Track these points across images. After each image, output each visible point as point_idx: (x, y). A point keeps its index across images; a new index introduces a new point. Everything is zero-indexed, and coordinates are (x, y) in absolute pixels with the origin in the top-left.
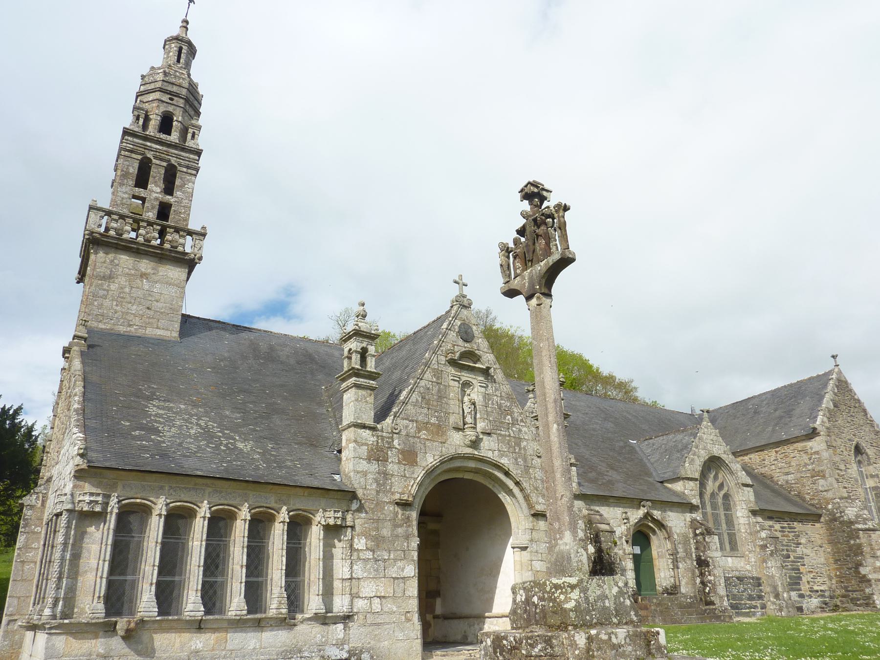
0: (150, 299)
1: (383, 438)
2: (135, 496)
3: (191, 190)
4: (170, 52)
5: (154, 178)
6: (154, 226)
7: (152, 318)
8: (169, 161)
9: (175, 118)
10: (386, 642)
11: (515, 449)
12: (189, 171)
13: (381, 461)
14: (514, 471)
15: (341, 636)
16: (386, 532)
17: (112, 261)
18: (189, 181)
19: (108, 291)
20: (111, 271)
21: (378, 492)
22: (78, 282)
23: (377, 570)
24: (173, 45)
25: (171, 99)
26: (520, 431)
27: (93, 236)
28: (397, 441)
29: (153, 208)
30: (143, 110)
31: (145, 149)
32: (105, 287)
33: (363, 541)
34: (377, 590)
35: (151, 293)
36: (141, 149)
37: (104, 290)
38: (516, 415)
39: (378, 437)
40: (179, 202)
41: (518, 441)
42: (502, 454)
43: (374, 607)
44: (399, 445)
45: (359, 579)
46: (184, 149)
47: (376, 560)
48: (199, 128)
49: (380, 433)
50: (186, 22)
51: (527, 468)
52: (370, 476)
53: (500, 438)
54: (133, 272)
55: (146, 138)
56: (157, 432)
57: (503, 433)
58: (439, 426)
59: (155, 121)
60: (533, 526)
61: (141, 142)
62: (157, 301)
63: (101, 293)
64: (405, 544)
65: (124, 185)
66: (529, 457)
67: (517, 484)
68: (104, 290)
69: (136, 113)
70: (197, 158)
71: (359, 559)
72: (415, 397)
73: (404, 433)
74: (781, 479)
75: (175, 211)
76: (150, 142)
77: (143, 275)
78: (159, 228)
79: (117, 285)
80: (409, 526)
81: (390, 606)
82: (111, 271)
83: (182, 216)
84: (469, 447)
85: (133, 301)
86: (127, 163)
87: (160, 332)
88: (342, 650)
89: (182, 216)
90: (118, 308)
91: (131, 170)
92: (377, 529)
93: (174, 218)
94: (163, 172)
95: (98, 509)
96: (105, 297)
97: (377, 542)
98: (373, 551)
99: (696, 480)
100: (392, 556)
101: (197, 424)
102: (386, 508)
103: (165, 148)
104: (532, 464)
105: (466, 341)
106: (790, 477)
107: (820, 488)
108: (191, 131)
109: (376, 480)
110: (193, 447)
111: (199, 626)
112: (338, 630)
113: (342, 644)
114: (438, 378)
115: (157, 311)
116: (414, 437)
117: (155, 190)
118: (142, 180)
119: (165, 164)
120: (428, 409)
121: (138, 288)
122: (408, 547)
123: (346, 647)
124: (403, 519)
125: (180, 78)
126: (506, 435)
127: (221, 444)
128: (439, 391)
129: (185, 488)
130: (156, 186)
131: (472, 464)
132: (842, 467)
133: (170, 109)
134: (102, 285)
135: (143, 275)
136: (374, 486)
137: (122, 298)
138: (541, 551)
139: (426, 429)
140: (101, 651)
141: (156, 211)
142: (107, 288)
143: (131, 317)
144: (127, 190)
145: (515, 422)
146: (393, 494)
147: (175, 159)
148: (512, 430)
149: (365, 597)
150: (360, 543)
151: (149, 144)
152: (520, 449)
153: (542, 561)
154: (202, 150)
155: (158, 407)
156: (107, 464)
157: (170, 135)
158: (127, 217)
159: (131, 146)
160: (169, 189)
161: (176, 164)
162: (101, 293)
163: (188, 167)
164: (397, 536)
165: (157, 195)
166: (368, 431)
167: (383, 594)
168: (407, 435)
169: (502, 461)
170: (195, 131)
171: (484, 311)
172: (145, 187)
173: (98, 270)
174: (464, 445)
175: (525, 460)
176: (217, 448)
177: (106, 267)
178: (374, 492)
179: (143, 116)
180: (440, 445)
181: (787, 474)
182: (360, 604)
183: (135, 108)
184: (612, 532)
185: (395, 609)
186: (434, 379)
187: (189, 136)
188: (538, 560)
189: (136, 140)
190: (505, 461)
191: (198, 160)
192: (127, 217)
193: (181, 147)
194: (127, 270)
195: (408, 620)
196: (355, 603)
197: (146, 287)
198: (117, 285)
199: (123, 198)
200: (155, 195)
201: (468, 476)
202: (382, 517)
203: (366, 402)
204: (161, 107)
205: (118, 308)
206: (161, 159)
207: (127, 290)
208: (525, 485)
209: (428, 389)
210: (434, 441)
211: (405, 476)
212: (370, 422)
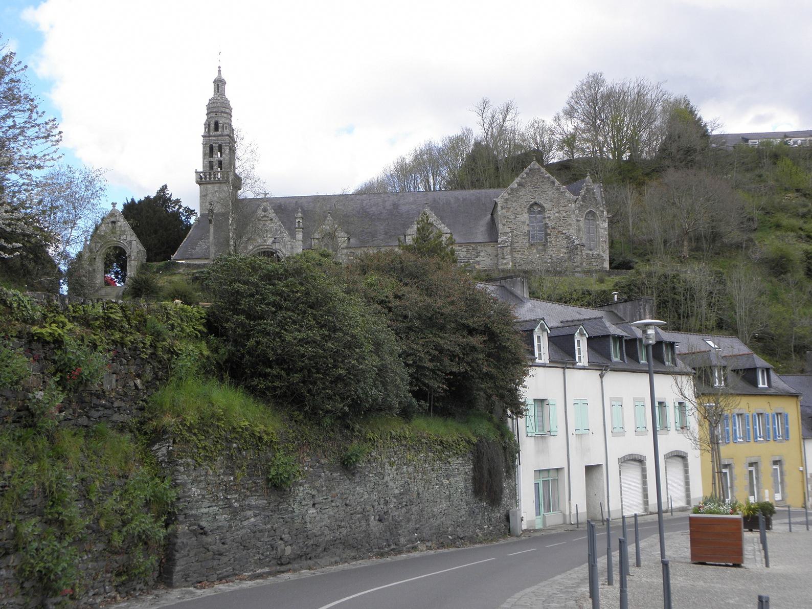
46: (223, 136)
51: (285, 246)
55: (209, 136)
59: (213, 126)
125: (218, 102)
133: (216, 119)
145: (281, 233)
160: (211, 163)
172: (212, 157)
208: (284, 251)
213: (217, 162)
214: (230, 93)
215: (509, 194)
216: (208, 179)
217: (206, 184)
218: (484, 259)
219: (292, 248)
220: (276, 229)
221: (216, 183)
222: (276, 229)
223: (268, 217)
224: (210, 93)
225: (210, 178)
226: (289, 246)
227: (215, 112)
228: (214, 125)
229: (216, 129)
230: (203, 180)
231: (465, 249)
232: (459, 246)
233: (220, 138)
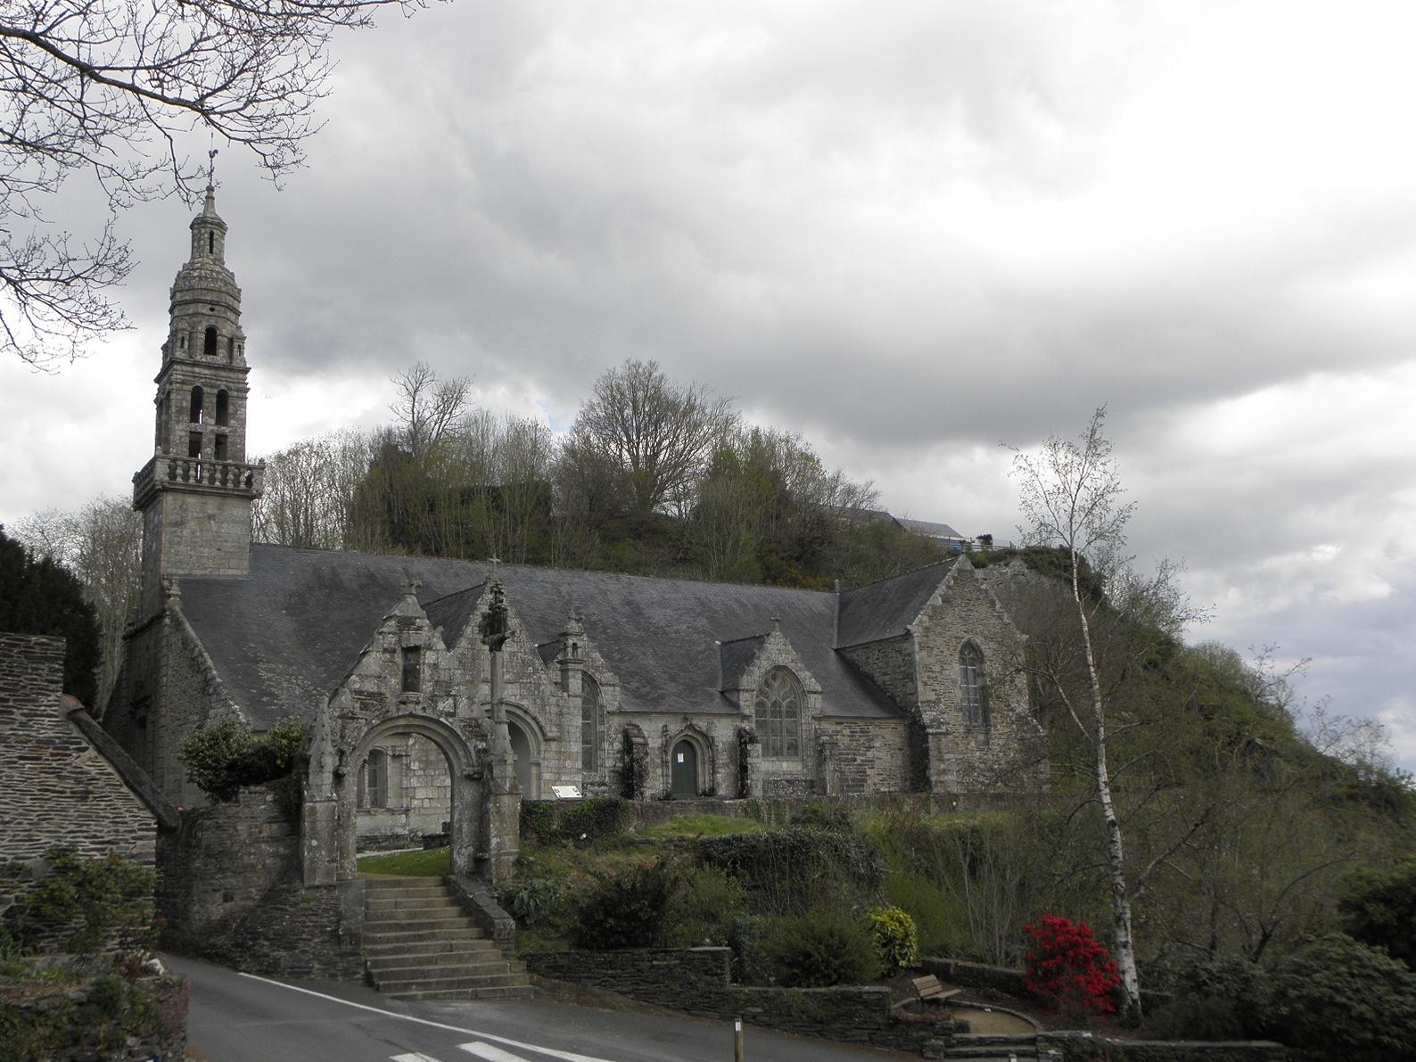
14: (532, 709)
15: (404, 821)
16: (432, 758)
17: (181, 507)
19: (181, 537)
24: (203, 231)
25: (212, 310)
29: (210, 442)
32: (179, 534)
33: (417, 764)
41: (538, 686)
46: (232, 370)
54: (201, 515)
55: (195, 364)
61: (190, 369)
62: (226, 541)
63: (176, 540)
67: (534, 719)
74: (880, 679)
77: (210, 517)
78: (220, 467)
86: (179, 397)
87: (231, 572)
90: (192, 553)
91: (185, 404)
92: (427, 756)
94: (215, 400)
96: (179, 543)
97: (427, 764)
99: (753, 691)
103: (213, 372)
106: (887, 678)
107: (908, 692)
108: (236, 344)
117: (207, 422)
119: (216, 391)
121: (207, 530)
125: (217, 279)
128: (473, 655)
130: (210, 417)
132: (937, 668)
133: (212, 322)
134: (175, 532)
135: (210, 517)
143: (205, 561)
145: (536, 671)
150: (415, 766)
151: (197, 370)
157: (215, 354)
162: (176, 540)
163: (238, 390)
171: (645, 364)
175: (542, 700)
181: (885, 674)
182: (415, 803)
184: (646, 744)
187: (236, 350)
189: (184, 368)
190: (525, 703)
193: (229, 368)
197: (214, 529)
200: (210, 428)
205: (192, 553)
206: (212, 386)
207: (198, 534)
213: (213, 437)
214: (237, 259)
215: (931, 618)
216: (205, 482)
217: (184, 492)
218: (881, 755)
219: (560, 714)
221: (211, 494)
225: (224, 482)
226: (554, 710)
227: (211, 303)
228: (203, 336)
229: (211, 347)
230: (179, 479)
231: (847, 732)
232: (837, 723)
233: (223, 374)
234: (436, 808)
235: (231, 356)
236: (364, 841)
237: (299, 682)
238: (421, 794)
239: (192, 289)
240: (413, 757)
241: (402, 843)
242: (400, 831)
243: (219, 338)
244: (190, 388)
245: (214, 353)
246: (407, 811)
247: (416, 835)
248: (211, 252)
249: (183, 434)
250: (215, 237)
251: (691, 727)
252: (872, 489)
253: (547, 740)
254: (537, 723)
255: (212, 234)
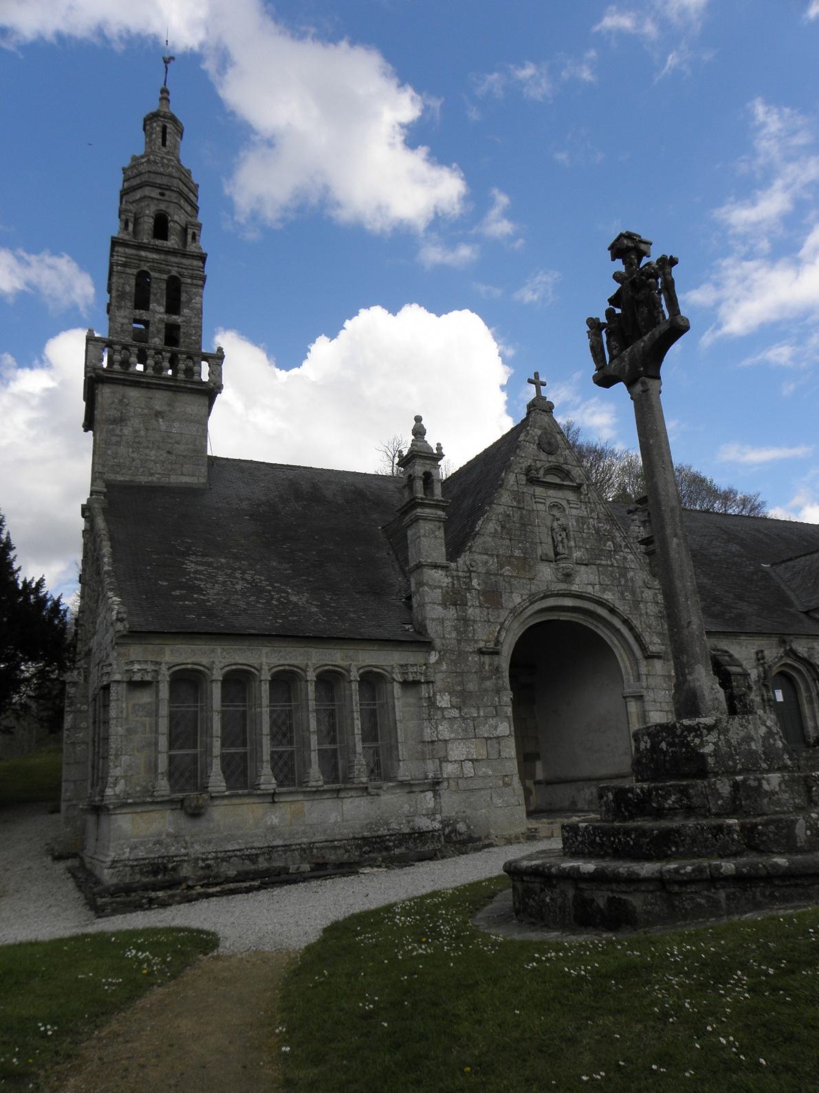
0: (170, 441)
1: (458, 577)
2: (185, 661)
3: (199, 306)
4: (152, 134)
5: (155, 295)
6: (164, 353)
7: (175, 463)
8: (169, 271)
9: (169, 218)
10: (483, 811)
11: (620, 582)
12: (195, 281)
13: (459, 605)
14: (621, 607)
15: (431, 804)
16: (471, 686)
17: (121, 401)
18: (196, 294)
20: (122, 413)
21: (459, 641)
22: (86, 430)
23: (465, 730)
25: (162, 194)
26: (625, 558)
27: (96, 374)
28: (476, 580)
29: (159, 331)
30: (131, 212)
31: (141, 260)
32: (118, 432)
33: (447, 697)
34: (468, 753)
35: (170, 434)
36: (135, 261)
37: (117, 436)
38: (618, 539)
39: (453, 577)
40: (188, 322)
41: (624, 571)
42: (604, 588)
43: (465, 772)
44: (479, 585)
45: (445, 741)
46: (184, 255)
47: (464, 719)
48: (199, 226)
49: (455, 573)
50: (164, 91)
51: (636, 604)
52: (448, 623)
53: (600, 569)
54: (146, 411)
55: (140, 247)
56: (200, 590)
57: (604, 562)
58: (525, 559)
59: (148, 224)
60: (648, 670)
61: (133, 252)
62: (178, 443)
63: (114, 439)
64: (496, 699)
65: (122, 307)
66: (638, 590)
67: (626, 622)
68: (117, 436)
69: (123, 217)
70: (201, 264)
71: (444, 718)
72: (492, 526)
73: (482, 570)
75: (184, 333)
76: (144, 251)
77: (158, 414)
79: (130, 428)
80: (499, 678)
81: (484, 770)
82: (122, 413)
83: (193, 338)
84: (562, 582)
85: (151, 445)
87: (185, 479)
88: (434, 820)
89: (193, 338)
90: (135, 455)
91: (128, 289)
92: (462, 683)
93: (184, 341)
94: (164, 286)
95: (148, 678)
96: (118, 444)
97: (463, 698)
98: (460, 709)
100: (482, 714)
101: (243, 579)
102: (470, 658)
103: (163, 257)
104: (642, 597)
105: (550, 453)
108: (190, 231)
109: (456, 628)
110: (242, 605)
111: (273, 797)
112: (428, 798)
113: (434, 814)
114: (519, 502)
115: (180, 455)
116: (496, 575)
117: (158, 310)
118: (142, 302)
119: (165, 277)
120: (510, 540)
121: (154, 429)
122: (500, 701)
123: (438, 817)
124: (491, 671)
126: (608, 566)
127: (272, 598)
128: (521, 517)
129: (240, 650)
130: (159, 304)
131: (568, 602)
133: (163, 206)
134: (113, 430)
135: (158, 414)
136: (454, 635)
137: (139, 443)
138: (659, 700)
139: (509, 564)
140: (171, 830)
141: (162, 336)
142: (119, 433)
143: (151, 465)
144: (126, 313)
146: (477, 641)
147: (176, 268)
148: (615, 558)
149: (455, 761)
150: (444, 701)
151: (143, 253)
152: (626, 581)
153: (661, 711)
154: (206, 254)
155: (196, 563)
156: (152, 628)
157: (166, 240)
158: (131, 346)
159: (124, 259)
160: (173, 306)
161: (177, 275)
162: (114, 439)
163: (192, 277)
164: (486, 690)
165: (161, 316)
166: (440, 572)
167: (475, 757)
168: (488, 573)
169: (605, 597)
170: (196, 231)
172: (146, 308)
173: (107, 413)
174: (556, 580)
175: (633, 593)
176: (268, 602)
177: (115, 409)
178: (454, 642)
179: (132, 219)
180: (528, 582)
182: (449, 769)
183: (121, 213)
185: (490, 773)
186: (515, 504)
187: (189, 238)
188: (657, 711)
189: (128, 251)
190: (608, 596)
191: (203, 268)
192: (131, 346)
194: (140, 410)
195: (506, 785)
196: (444, 768)
197: (163, 428)
198: (130, 428)
199: (122, 324)
200: (159, 316)
201: (564, 616)
202: (466, 669)
203: (436, 537)
204: (152, 207)
205: (135, 455)
206: (161, 271)
207: (142, 433)
208: (635, 622)
209: (508, 516)
210: (520, 578)
211: (489, 621)
212: (442, 560)
213: (162, 326)
220: (598, 531)
221: (159, 387)
222: (598, 531)
223: (567, 475)
224: (136, 144)
227: (160, 187)
228: (152, 221)
234: (486, 776)
235: (185, 243)
236: (359, 847)
237: (248, 577)
238: (457, 751)
239: (140, 174)
240: (439, 684)
241: (429, 847)
242: (424, 824)
243: (171, 224)
244: (135, 271)
245: (165, 238)
246: (435, 785)
247: (455, 831)
248: (164, 144)
249: (126, 321)
250: (168, 130)
251: (792, 653)
252: (760, 499)
253: (649, 657)
254: (631, 629)
255: (164, 129)
